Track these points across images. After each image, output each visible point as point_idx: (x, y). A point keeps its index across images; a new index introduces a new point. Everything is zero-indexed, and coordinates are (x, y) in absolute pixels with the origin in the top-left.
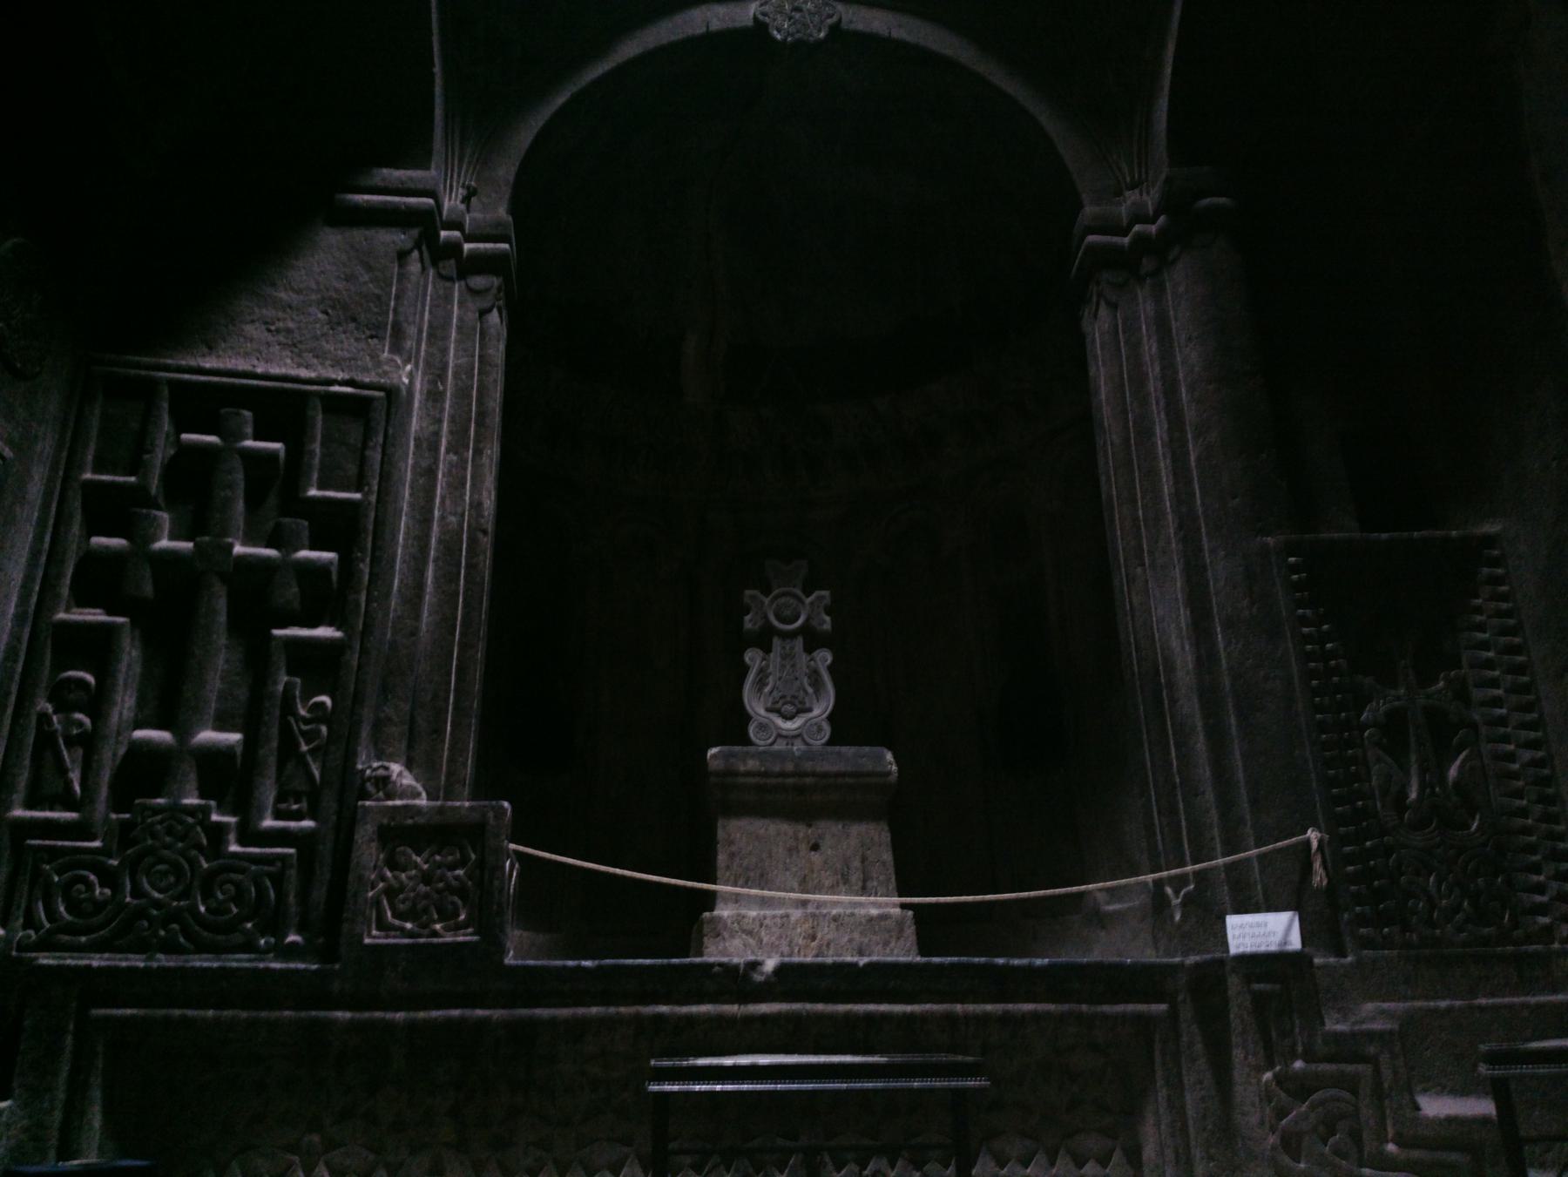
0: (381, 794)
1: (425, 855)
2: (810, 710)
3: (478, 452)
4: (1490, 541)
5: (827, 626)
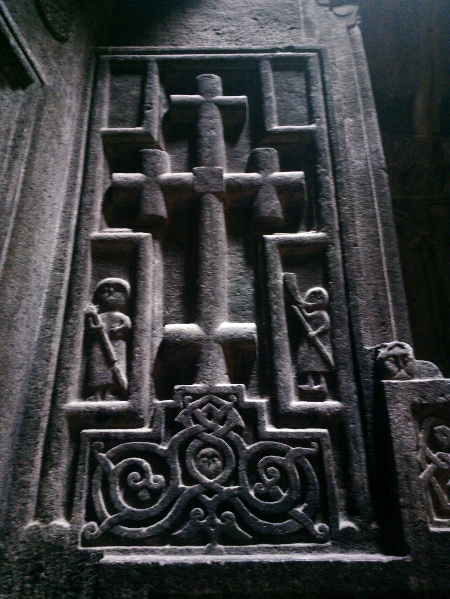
0: (403, 372)
3: (367, 114)
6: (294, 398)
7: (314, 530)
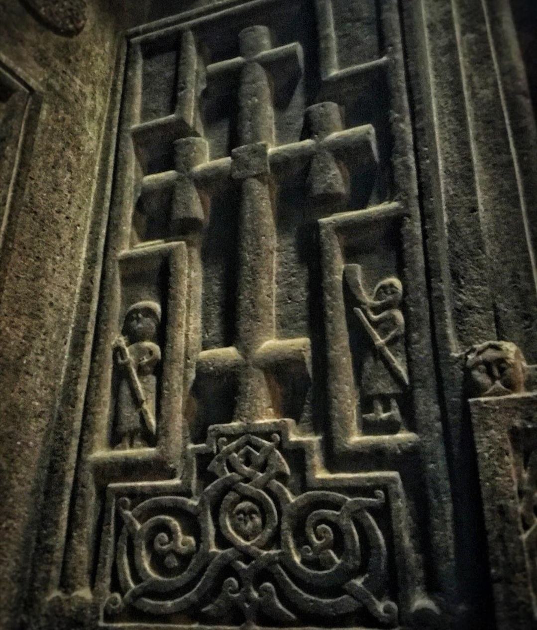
6: (356, 432)
7: (379, 612)
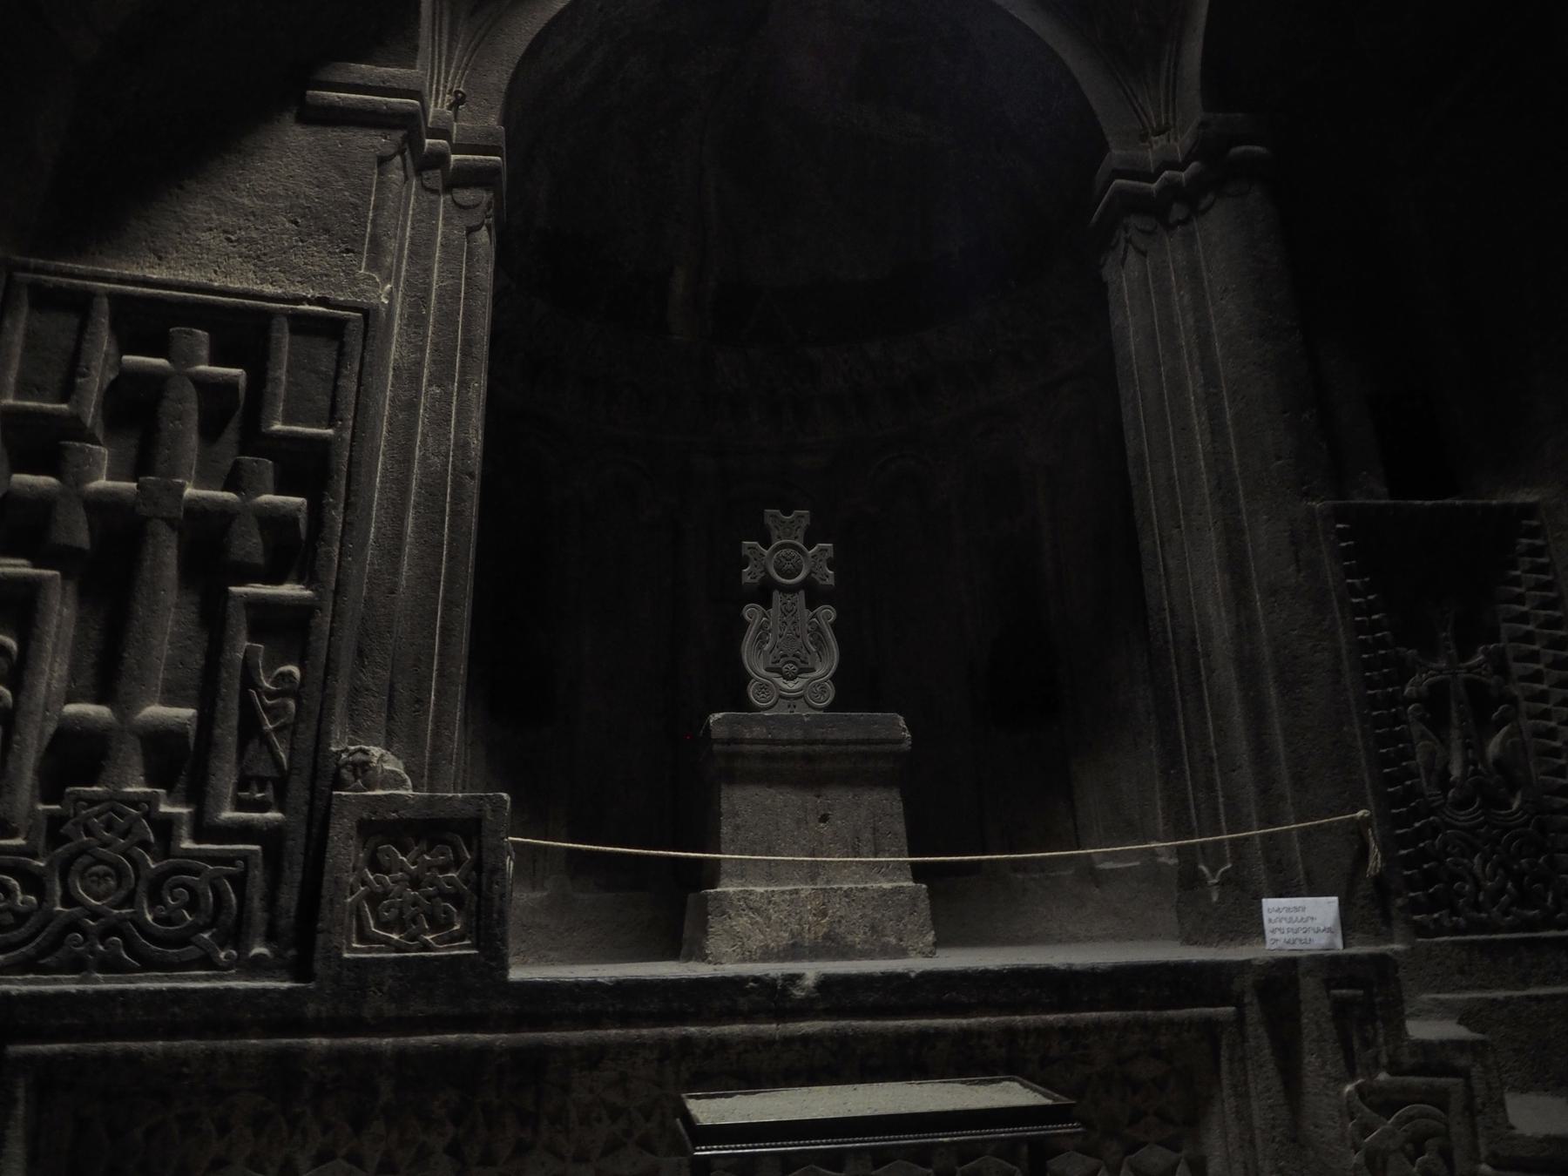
1: (412, 854)
2: (813, 670)
3: (464, 385)
4: (1529, 510)
5: (830, 581)
